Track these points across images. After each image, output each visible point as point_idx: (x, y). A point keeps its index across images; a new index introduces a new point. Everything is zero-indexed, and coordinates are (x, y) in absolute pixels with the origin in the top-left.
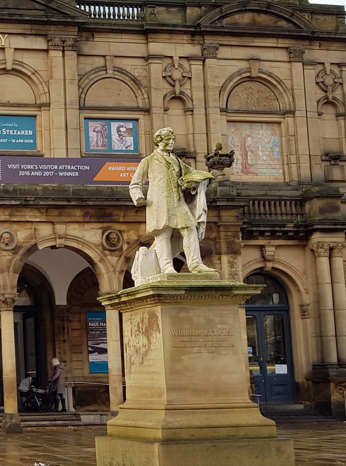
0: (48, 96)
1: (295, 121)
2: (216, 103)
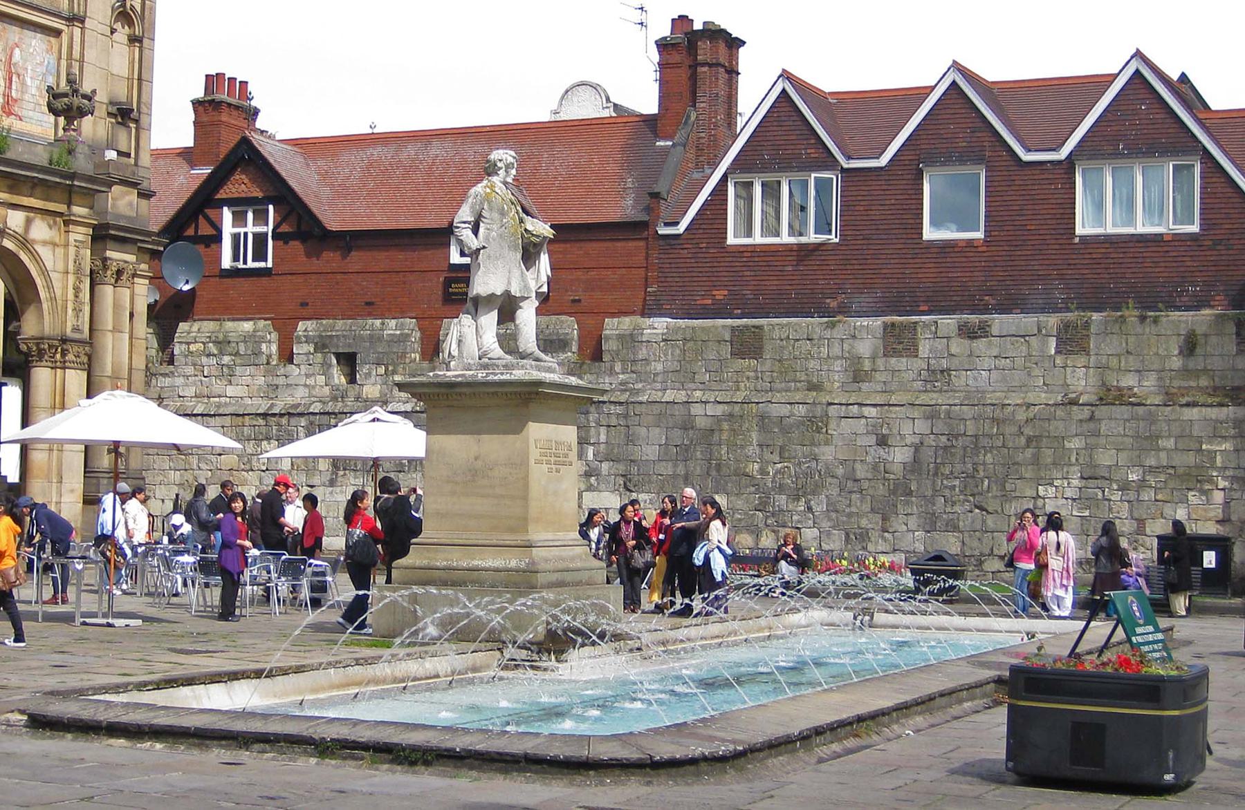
1: (83, 34)
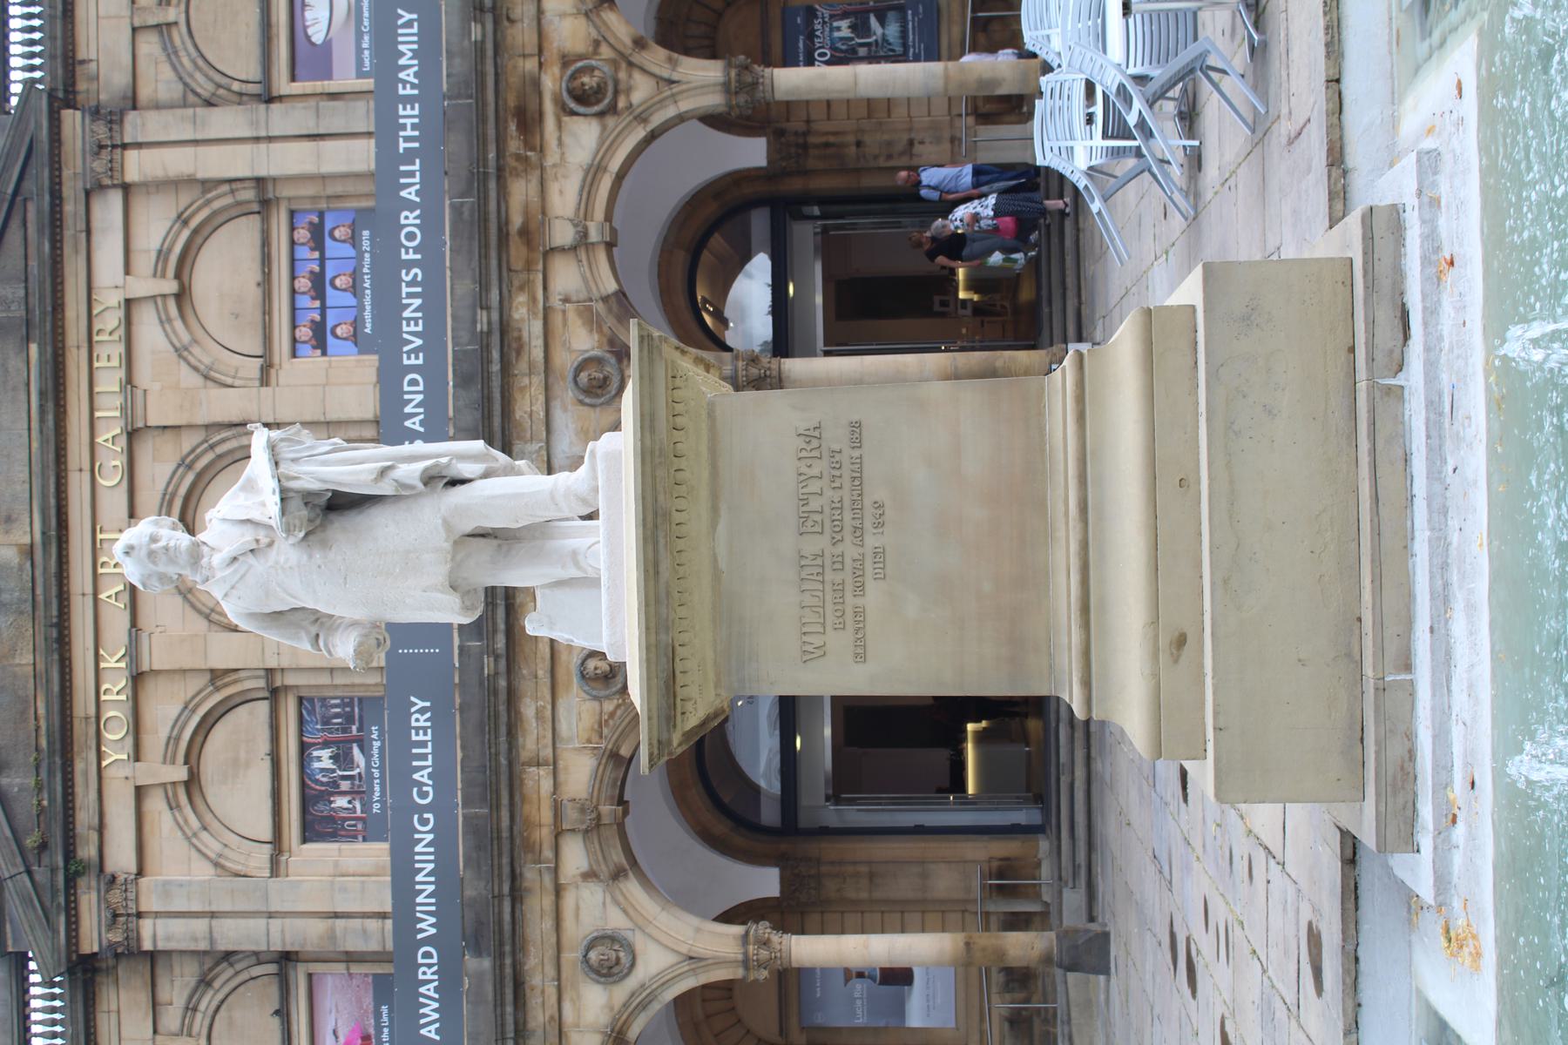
0: (239, 185)
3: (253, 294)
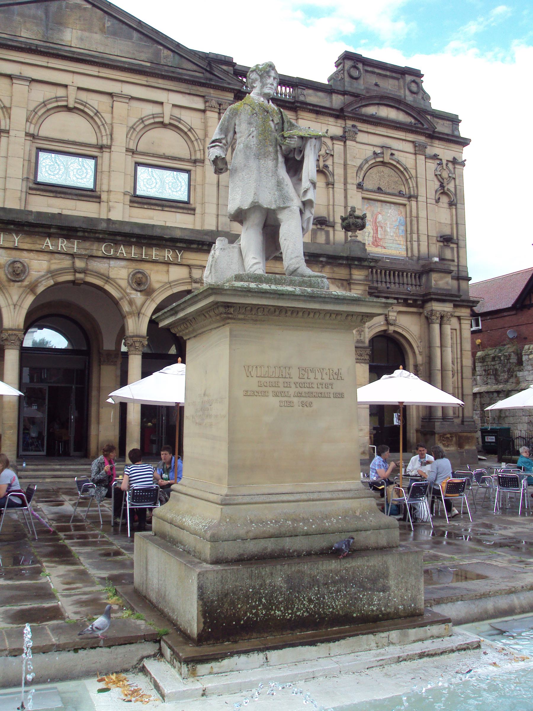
1: (417, 204)
2: (353, 180)
3: (161, 151)
